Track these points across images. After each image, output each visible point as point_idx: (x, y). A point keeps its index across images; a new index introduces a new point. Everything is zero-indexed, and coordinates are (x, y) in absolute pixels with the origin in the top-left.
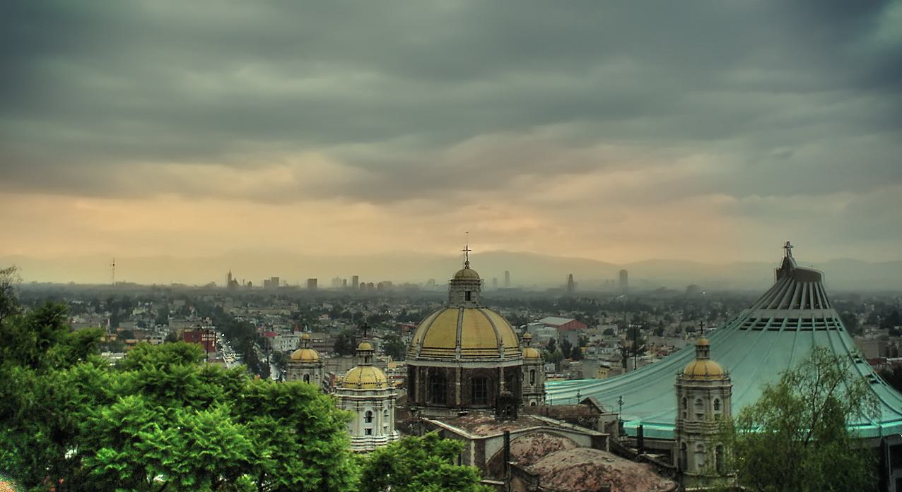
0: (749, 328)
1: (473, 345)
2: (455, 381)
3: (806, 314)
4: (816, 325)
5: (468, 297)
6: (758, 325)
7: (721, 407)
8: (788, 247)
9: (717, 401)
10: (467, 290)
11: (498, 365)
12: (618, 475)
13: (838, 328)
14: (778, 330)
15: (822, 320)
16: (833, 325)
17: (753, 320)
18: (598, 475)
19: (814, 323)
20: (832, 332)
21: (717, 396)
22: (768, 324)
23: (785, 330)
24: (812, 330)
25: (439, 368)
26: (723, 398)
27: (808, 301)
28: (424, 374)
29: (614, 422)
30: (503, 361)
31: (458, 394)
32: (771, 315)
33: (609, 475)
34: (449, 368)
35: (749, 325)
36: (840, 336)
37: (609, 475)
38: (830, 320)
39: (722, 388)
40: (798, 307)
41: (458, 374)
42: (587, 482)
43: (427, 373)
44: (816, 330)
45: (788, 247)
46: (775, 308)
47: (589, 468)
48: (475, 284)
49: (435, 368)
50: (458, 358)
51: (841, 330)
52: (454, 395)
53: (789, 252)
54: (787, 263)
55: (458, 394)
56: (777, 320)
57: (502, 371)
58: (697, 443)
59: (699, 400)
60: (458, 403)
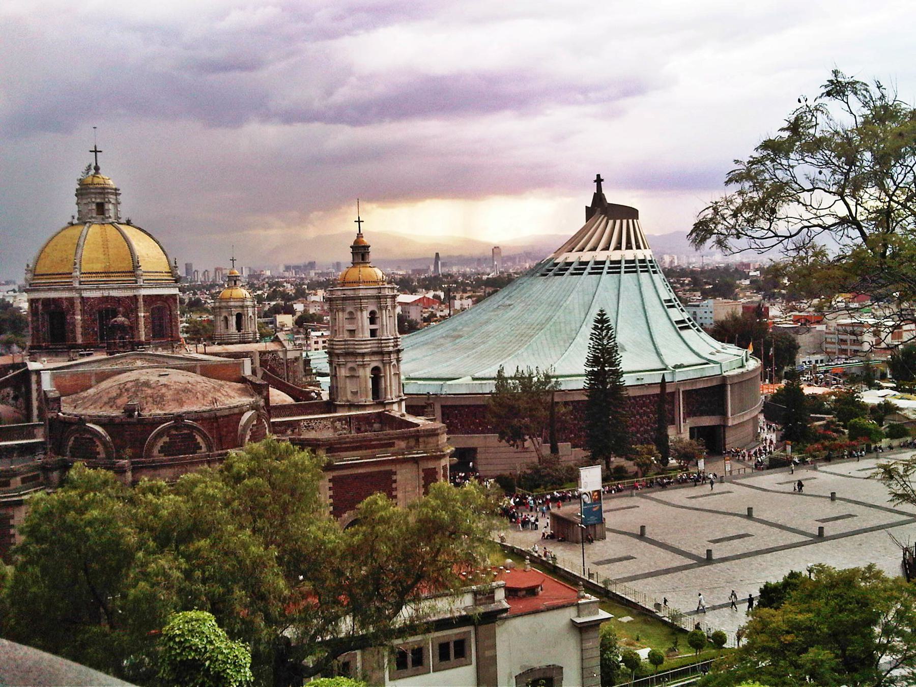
0: (551, 273)
1: (98, 267)
2: (74, 314)
3: (616, 255)
4: (626, 267)
6: (560, 270)
7: (378, 321)
8: (599, 180)
9: (372, 313)
10: (98, 201)
11: (136, 292)
13: (651, 270)
14: (582, 274)
15: (633, 261)
16: (646, 267)
19: (623, 265)
20: (644, 277)
21: (372, 308)
22: (572, 268)
23: (590, 273)
24: (619, 272)
25: (53, 299)
26: (381, 309)
28: (37, 308)
29: (296, 359)
30: (141, 287)
31: (79, 330)
33: (149, 391)
34: (66, 299)
35: (550, 270)
36: (653, 281)
37: (149, 391)
38: (643, 261)
39: (378, 298)
41: (78, 306)
43: (40, 307)
44: (626, 272)
45: (599, 180)
47: (129, 385)
48: (112, 194)
49: (49, 299)
50: (76, 285)
51: (655, 272)
52: (73, 331)
53: (599, 188)
54: (599, 198)
55: (79, 330)
57: (141, 300)
58: (350, 365)
59: (351, 313)
60: (80, 341)
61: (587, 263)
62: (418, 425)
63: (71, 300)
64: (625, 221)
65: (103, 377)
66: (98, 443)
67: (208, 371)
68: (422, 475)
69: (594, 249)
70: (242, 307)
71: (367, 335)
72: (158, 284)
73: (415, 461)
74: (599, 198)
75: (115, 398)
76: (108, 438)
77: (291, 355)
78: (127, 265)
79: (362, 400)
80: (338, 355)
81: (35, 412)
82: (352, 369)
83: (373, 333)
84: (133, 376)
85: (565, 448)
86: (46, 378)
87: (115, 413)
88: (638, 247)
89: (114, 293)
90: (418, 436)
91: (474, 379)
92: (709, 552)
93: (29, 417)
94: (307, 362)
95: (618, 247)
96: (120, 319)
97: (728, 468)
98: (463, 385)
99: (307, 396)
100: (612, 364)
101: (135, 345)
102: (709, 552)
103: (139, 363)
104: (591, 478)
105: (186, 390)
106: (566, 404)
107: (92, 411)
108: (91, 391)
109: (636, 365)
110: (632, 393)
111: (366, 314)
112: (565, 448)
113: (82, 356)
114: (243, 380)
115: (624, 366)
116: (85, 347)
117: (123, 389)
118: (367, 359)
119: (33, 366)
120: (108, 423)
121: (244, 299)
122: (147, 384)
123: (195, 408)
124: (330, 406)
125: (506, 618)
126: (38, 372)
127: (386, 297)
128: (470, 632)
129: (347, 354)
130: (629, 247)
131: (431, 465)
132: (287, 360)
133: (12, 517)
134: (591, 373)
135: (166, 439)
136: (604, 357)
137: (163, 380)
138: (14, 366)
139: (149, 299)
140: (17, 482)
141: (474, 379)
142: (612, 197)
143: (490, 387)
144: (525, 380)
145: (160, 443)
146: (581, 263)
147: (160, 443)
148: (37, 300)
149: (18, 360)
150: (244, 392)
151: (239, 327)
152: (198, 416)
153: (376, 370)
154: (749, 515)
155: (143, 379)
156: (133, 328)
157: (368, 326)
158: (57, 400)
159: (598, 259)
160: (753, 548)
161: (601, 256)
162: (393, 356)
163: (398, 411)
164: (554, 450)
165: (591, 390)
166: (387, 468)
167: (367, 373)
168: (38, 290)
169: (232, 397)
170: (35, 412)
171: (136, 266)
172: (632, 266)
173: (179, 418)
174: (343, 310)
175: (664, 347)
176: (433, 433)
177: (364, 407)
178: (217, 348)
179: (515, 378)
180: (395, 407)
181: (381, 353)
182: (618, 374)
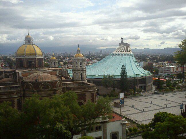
3: (125, 53)
5: (29, 42)
7: (82, 64)
9: (81, 63)
19: (127, 55)
20: (131, 57)
25: (21, 59)
26: (82, 62)
27: (126, 50)
29: (66, 71)
32: (117, 53)
39: (82, 60)
41: (25, 59)
47: (36, 76)
53: (122, 40)
54: (122, 42)
57: (37, 59)
58: (76, 73)
61: (120, 54)
62: (90, 85)
63: (24, 59)
65: (31, 74)
66: (30, 86)
67: (50, 73)
68: (91, 94)
69: (121, 51)
70: (55, 61)
71: (80, 67)
72: (40, 56)
73: (90, 92)
74: (122, 42)
76: (32, 86)
77: (65, 70)
78: (34, 53)
79: (78, 79)
80: (74, 71)
81: (18, 80)
82: (77, 73)
83: (81, 67)
84: (36, 74)
85: (116, 89)
86: (20, 74)
87: (33, 81)
88: (130, 51)
89: (32, 58)
90: (90, 87)
91: (98, 76)
92: (144, 110)
93: (16, 81)
94: (68, 71)
95: (126, 51)
96: (33, 63)
97: (147, 94)
98: (97, 76)
99: (68, 78)
101: (36, 68)
102: (144, 110)
103: (37, 71)
104: (122, 95)
105: (47, 77)
106: (116, 81)
107: (29, 80)
108: (29, 76)
109: (130, 73)
110: (129, 79)
111: (80, 63)
112: (116, 89)
113: (26, 69)
114: (57, 75)
115: (127, 74)
116: (26, 68)
117: (35, 76)
118: (80, 72)
119: (17, 71)
120: (32, 83)
121: (55, 59)
122: (39, 75)
123: (48, 80)
124: (72, 80)
125: (108, 122)
126: (18, 72)
127: (83, 60)
128: (101, 125)
129: (76, 71)
131: (93, 93)
132: (64, 71)
133: (14, 100)
135: (43, 86)
136: (124, 72)
137: (42, 75)
138: (13, 71)
140: (15, 93)
141: (98, 76)
142: (125, 41)
143: (102, 77)
144: (109, 76)
145: (42, 87)
146: (119, 54)
149: (14, 70)
150: (57, 77)
151: (54, 65)
152: (49, 82)
153: (81, 74)
154: (151, 103)
155: (38, 74)
156: (35, 64)
157: (80, 65)
158: (23, 78)
159: (122, 53)
160: (152, 109)
161: (122, 53)
162: (85, 71)
163: (86, 82)
164: (114, 89)
165: (121, 78)
166: (84, 93)
167: (80, 74)
168: (17, 57)
169: (55, 78)
170: (18, 80)
171: (36, 52)
172: (128, 55)
173: (46, 82)
174: (75, 62)
175: (135, 70)
176: (93, 86)
177: (79, 81)
178: (51, 69)
180: (85, 81)
181: (82, 71)
182: (126, 75)
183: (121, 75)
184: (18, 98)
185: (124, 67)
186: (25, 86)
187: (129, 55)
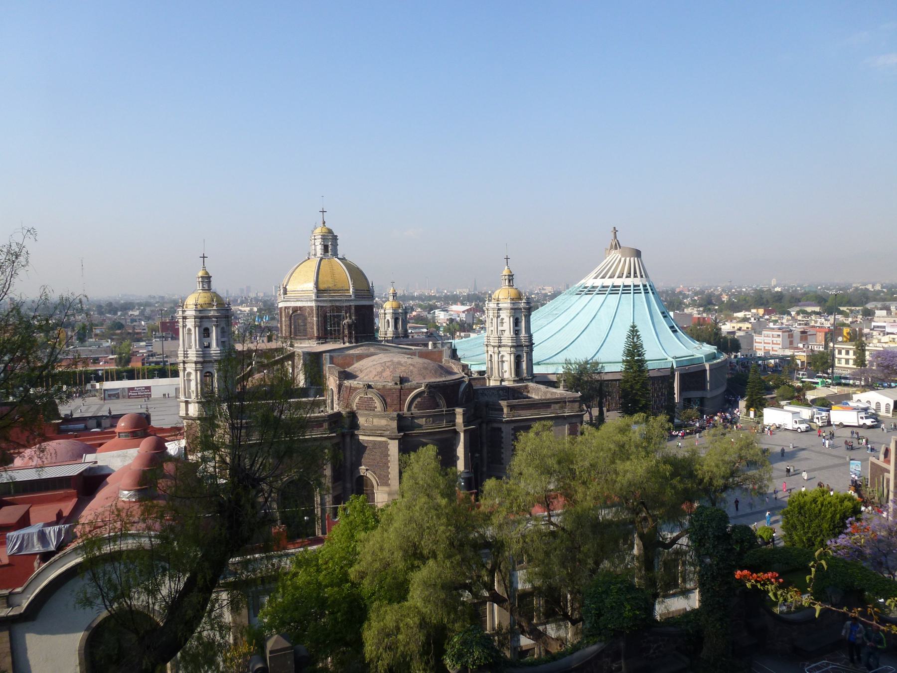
8: (615, 231)
12: (411, 368)
17: (586, 288)
18: (394, 369)
25: (300, 307)
33: (403, 368)
37: (403, 368)
40: (621, 277)
42: (384, 374)
45: (615, 231)
46: (603, 277)
47: (388, 364)
56: (603, 287)
61: (608, 287)
64: (628, 259)
75: (381, 372)
100: (639, 355)
110: (652, 374)
115: (647, 357)
122: (399, 363)
130: (635, 276)
134: (627, 361)
136: (634, 351)
139: (357, 307)
147: (416, 402)
148: (289, 308)
179: (575, 363)
183: (624, 361)
184: (335, 441)
185: (637, 331)
186: (357, 400)
187: (641, 287)
